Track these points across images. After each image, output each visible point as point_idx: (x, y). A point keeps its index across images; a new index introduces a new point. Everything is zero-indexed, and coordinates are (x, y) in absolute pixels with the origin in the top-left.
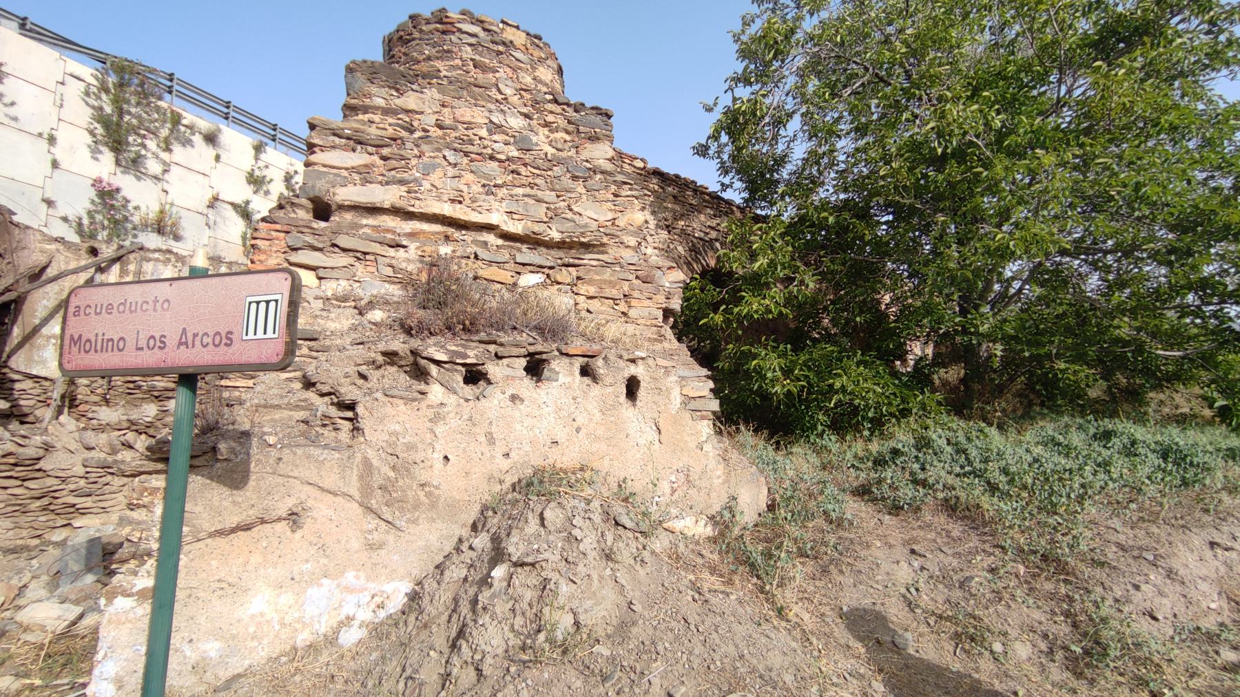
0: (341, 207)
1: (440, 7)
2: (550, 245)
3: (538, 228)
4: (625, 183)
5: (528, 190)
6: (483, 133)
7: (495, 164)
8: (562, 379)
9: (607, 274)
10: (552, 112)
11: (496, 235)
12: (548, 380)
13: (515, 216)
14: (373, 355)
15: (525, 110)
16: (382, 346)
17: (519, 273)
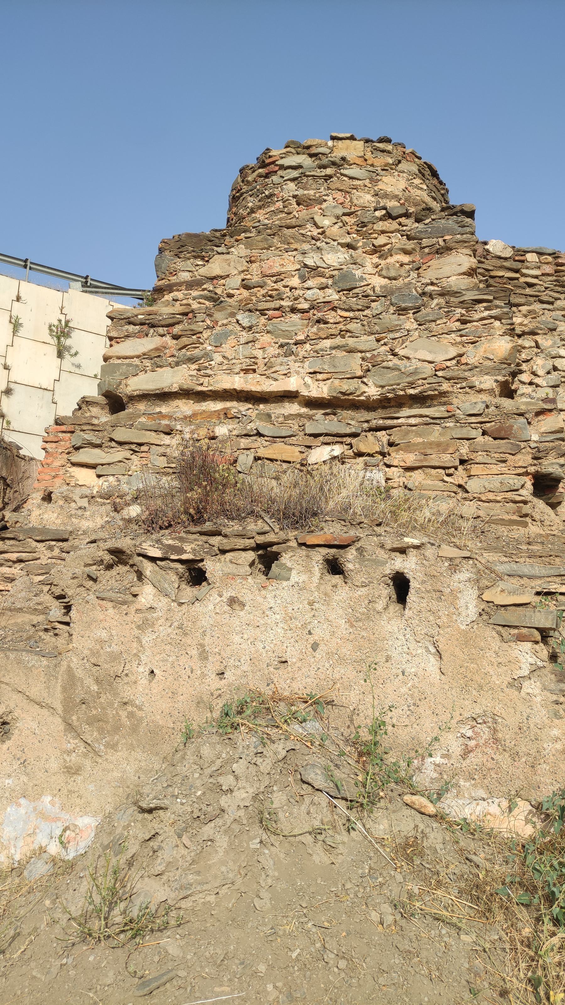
0: (132, 398)
1: (263, 150)
2: (368, 406)
3: (346, 386)
4: (480, 301)
5: (338, 341)
6: (295, 281)
7: (296, 317)
8: (295, 577)
9: (435, 434)
10: (383, 232)
11: (300, 404)
12: (276, 578)
13: (320, 377)
14: (101, 553)
15: (347, 240)
16: (110, 544)
17: (309, 447)
